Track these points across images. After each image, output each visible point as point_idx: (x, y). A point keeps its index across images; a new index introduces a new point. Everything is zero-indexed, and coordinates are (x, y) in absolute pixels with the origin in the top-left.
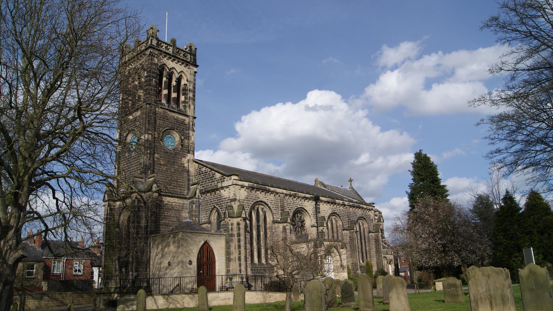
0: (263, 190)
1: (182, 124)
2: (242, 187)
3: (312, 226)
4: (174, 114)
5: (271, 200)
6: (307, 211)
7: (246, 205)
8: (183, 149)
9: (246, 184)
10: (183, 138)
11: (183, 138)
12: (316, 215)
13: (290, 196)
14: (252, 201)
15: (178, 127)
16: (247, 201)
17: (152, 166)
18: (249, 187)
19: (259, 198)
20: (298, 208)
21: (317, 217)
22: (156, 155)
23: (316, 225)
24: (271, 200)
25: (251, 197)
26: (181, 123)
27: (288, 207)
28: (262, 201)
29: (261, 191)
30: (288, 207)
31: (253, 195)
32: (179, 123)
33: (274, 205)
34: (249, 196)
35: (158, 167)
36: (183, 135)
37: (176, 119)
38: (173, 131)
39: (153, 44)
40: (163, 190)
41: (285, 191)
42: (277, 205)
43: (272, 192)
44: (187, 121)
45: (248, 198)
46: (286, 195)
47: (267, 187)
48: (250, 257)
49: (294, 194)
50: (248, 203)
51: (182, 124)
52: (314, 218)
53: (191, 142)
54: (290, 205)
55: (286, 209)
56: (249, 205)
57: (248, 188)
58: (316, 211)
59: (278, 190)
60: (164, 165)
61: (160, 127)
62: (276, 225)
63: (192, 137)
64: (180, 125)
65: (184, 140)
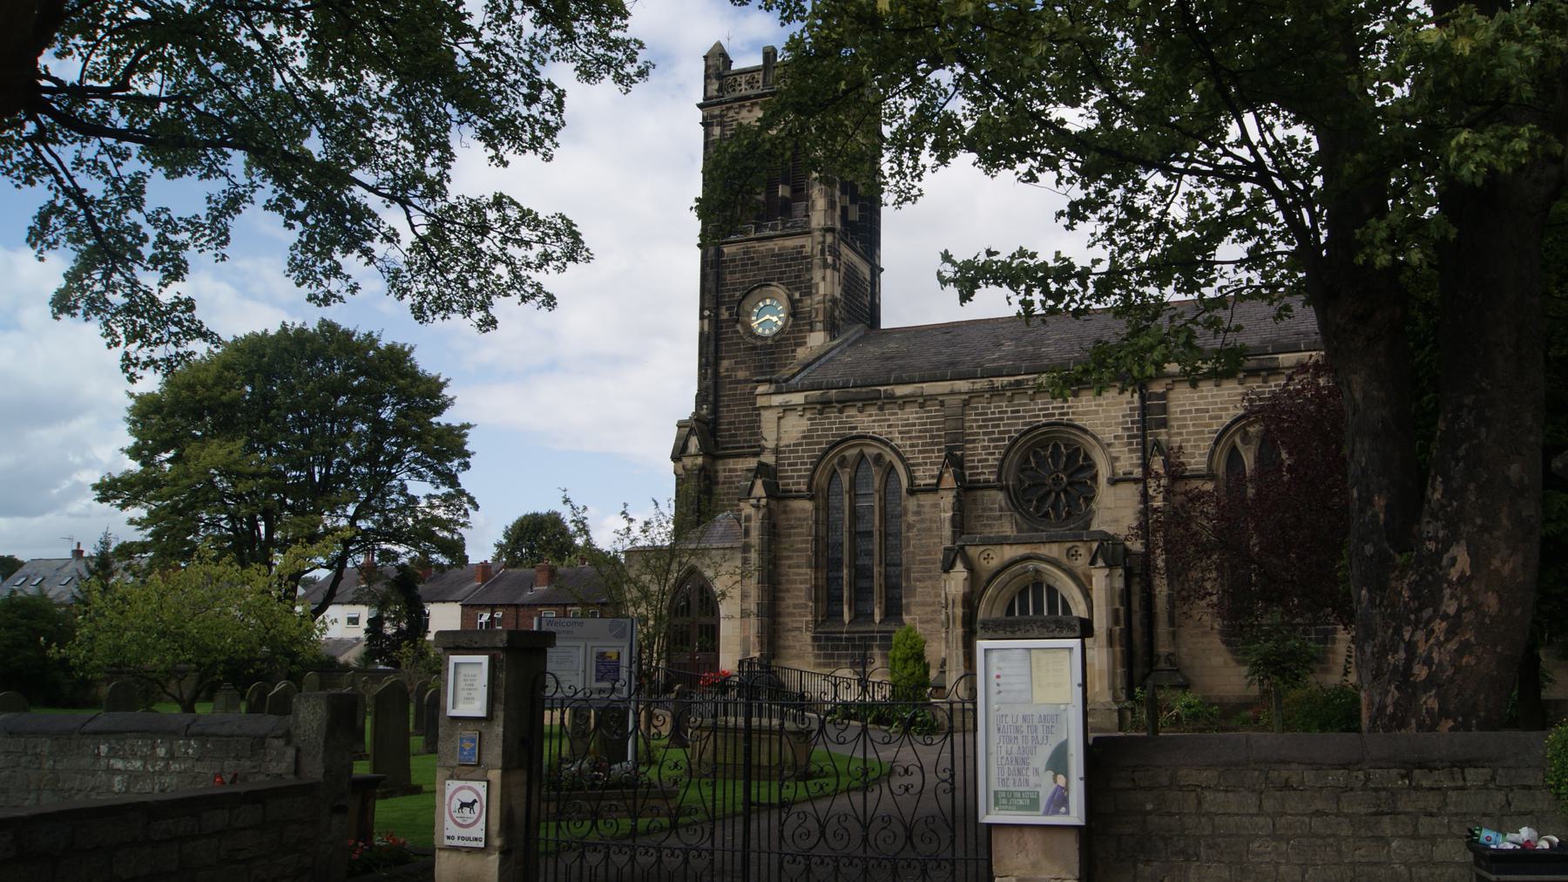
0: (867, 401)
1: (796, 259)
2: (787, 409)
3: (1114, 481)
4: (770, 245)
5: (907, 425)
6: (1085, 431)
7: (803, 457)
8: (799, 325)
9: (798, 398)
10: (797, 295)
11: (797, 295)
12: (1144, 437)
13: (995, 392)
14: (827, 443)
15: (785, 272)
16: (807, 444)
17: (711, 391)
18: (807, 403)
19: (855, 428)
20: (1038, 427)
21: (1144, 443)
22: (725, 364)
23: (1138, 473)
24: (907, 425)
25: (823, 430)
26: (792, 259)
27: (984, 434)
28: (865, 437)
29: (860, 404)
30: (984, 434)
31: (835, 423)
32: (786, 260)
33: (920, 437)
34: (817, 430)
35: (730, 389)
36: (797, 289)
37: (777, 255)
38: (772, 288)
39: (709, 94)
40: (745, 441)
41: (963, 385)
42: (932, 437)
43: (906, 401)
44: (808, 249)
45: (812, 437)
46: (973, 394)
47: (882, 388)
48: (811, 604)
49: (1010, 384)
50: (814, 450)
51: (796, 259)
52: (1131, 451)
53: (817, 298)
54: (998, 426)
55: (973, 441)
56: (815, 456)
57: (807, 406)
58: (1144, 421)
59: (929, 388)
60: (746, 381)
61: (734, 290)
62: (926, 500)
63: (822, 285)
64: (790, 266)
65: (800, 301)
